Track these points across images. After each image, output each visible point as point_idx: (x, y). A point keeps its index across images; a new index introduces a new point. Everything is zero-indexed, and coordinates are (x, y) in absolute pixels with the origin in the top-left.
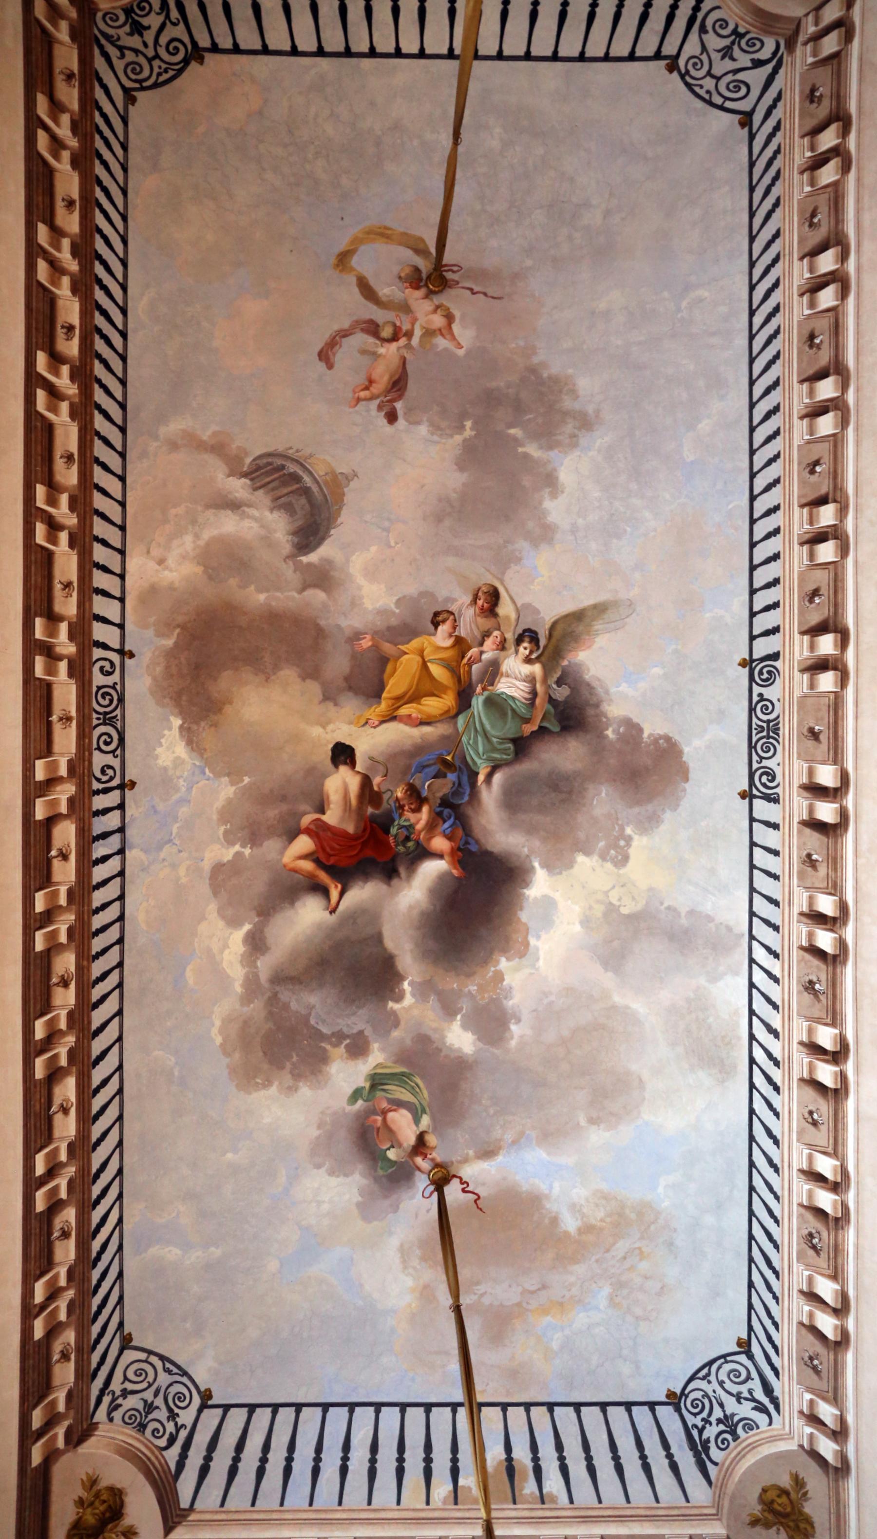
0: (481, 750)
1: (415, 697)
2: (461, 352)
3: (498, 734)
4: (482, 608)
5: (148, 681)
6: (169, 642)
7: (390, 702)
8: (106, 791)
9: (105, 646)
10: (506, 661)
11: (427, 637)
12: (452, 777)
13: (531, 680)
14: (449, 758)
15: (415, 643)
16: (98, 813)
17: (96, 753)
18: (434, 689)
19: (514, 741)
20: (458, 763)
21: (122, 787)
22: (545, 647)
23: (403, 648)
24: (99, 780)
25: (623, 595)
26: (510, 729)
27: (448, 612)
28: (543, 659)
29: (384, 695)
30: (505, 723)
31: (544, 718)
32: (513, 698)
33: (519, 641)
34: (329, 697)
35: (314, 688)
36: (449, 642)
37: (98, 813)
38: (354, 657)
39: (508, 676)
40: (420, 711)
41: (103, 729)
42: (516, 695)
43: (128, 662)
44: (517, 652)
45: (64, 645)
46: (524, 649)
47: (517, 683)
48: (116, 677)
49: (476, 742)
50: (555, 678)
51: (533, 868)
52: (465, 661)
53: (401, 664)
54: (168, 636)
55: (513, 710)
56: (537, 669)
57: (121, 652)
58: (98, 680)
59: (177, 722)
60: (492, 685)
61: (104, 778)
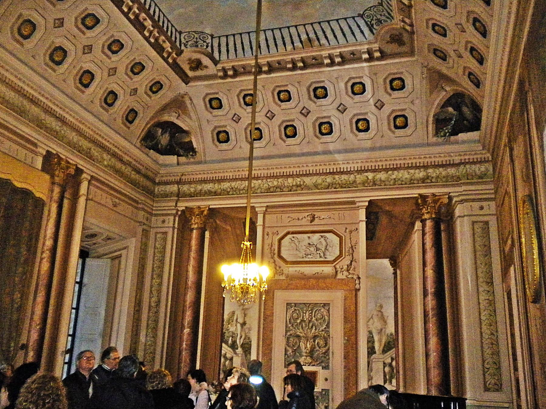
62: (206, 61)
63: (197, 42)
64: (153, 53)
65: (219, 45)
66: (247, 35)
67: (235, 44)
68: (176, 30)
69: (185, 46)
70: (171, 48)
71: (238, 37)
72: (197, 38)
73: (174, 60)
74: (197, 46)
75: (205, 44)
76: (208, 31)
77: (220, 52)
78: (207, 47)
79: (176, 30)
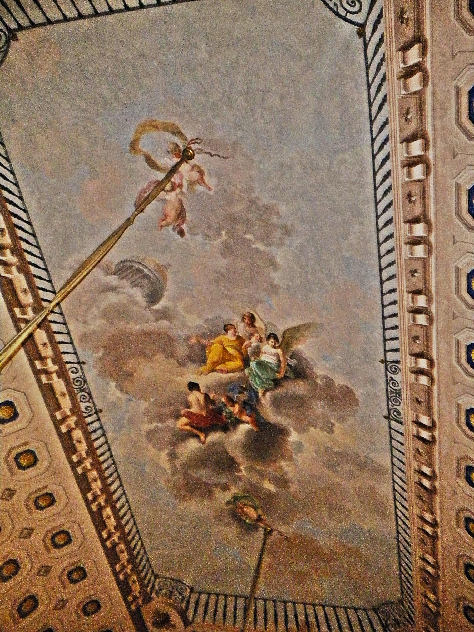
0: (258, 383)
1: (222, 361)
2: (211, 193)
3: (266, 377)
4: (248, 324)
5: (95, 371)
6: (100, 354)
7: (211, 365)
8: (90, 416)
9: (70, 363)
10: (264, 347)
11: (223, 336)
12: (247, 394)
13: (277, 355)
14: (244, 386)
15: (218, 339)
16: (89, 424)
17: (81, 404)
18: (231, 358)
19: (273, 381)
20: (248, 388)
21: (96, 412)
22: (282, 342)
23: (213, 341)
24: (86, 413)
25: (318, 321)
26: (271, 375)
27: (231, 325)
28: (282, 346)
29: (208, 362)
30: (268, 372)
31: (286, 372)
32: (269, 363)
33: (268, 338)
34: (181, 364)
35: (173, 362)
36: (234, 338)
37: (89, 424)
38: (189, 347)
39: (265, 353)
40: (227, 368)
41: (81, 394)
42: (271, 361)
43: (84, 366)
44: (268, 344)
45: (51, 366)
46: (272, 341)
47: (271, 357)
48: (80, 373)
49: (255, 380)
50: (289, 356)
51: (289, 430)
52: (243, 346)
53: (213, 348)
54: (99, 351)
55: (271, 368)
56: (279, 351)
57: (79, 363)
58: (72, 376)
59: (113, 384)
60: (258, 357)
61: (88, 411)
62: (175, 618)
63: (171, 592)
64: (117, 593)
65: (197, 603)
66: (234, 598)
67: (216, 606)
68: (153, 572)
69: (157, 593)
70: (140, 592)
71: (222, 598)
72: (173, 588)
73: (138, 608)
74: (170, 597)
75: (181, 597)
76: (189, 581)
77: (195, 611)
78: (182, 600)
79: (153, 572)
